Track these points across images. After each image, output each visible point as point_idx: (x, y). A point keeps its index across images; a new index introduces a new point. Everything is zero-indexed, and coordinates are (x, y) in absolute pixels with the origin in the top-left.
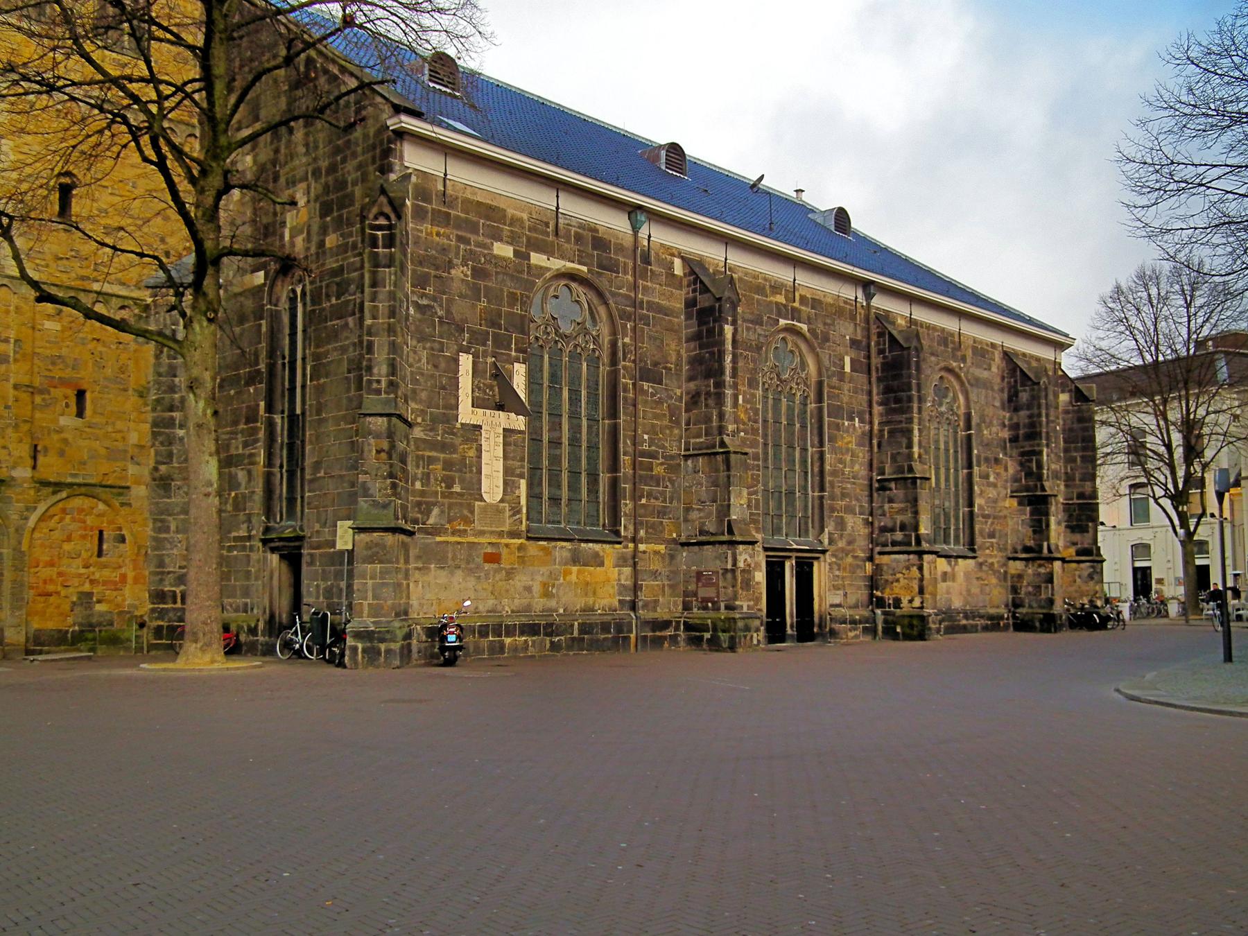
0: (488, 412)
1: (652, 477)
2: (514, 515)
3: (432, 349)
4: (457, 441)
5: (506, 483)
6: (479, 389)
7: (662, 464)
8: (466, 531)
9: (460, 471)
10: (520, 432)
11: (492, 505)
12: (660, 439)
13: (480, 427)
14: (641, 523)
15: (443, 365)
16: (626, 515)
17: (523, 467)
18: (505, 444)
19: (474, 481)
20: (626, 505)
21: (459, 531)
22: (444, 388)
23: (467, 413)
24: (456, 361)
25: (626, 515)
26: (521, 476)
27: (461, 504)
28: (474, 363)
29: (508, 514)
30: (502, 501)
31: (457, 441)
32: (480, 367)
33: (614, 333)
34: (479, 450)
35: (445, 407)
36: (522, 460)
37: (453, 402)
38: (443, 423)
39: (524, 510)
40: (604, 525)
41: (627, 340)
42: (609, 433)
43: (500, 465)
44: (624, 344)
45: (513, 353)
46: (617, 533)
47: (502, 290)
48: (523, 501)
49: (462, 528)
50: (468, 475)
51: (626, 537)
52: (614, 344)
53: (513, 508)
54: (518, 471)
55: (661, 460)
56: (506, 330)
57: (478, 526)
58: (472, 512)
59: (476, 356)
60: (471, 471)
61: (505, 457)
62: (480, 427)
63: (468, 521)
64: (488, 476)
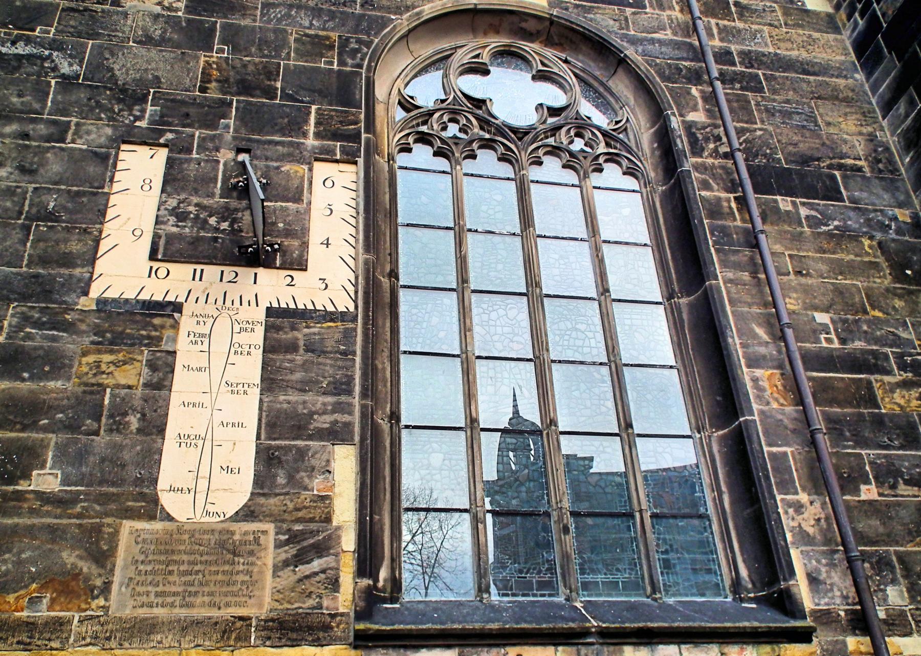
0: (213, 272)
1: (879, 422)
2: (300, 558)
3: (26, 136)
4: (69, 344)
5: (267, 459)
6: (181, 216)
7: (906, 385)
8: (58, 626)
9: (72, 427)
10: (343, 316)
11: (196, 533)
12: (875, 322)
13: (178, 307)
14: (882, 564)
15: (55, 166)
16: (804, 538)
17: (344, 408)
18: (270, 348)
19: (126, 456)
20: (799, 507)
21: (30, 626)
22: (50, 217)
23: (123, 268)
24: (105, 160)
25: (804, 538)
26: (337, 435)
27: (55, 534)
28: (170, 163)
29: (270, 556)
30: (248, 513)
31: (69, 344)
32: (191, 170)
33: (658, 115)
34: (163, 370)
35: (44, 260)
36: (342, 387)
37: (75, 246)
38: (24, 297)
39: (349, 542)
40: (737, 585)
41: (698, 116)
42: (694, 327)
43: (247, 409)
44: (689, 127)
45: (311, 142)
46: (785, 603)
47: (281, 34)
48: (345, 511)
49: (43, 612)
50: (102, 440)
51: (825, 617)
52: (664, 137)
53: (294, 538)
54: (323, 422)
55: (899, 376)
56: (285, 96)
57: (121, 603)
58: (103, 557)
59: (179, 148)
60: (118, 427)
61: (270, 381)
62: (178, 307)
63: (68, 587)
64: (184, 440)
